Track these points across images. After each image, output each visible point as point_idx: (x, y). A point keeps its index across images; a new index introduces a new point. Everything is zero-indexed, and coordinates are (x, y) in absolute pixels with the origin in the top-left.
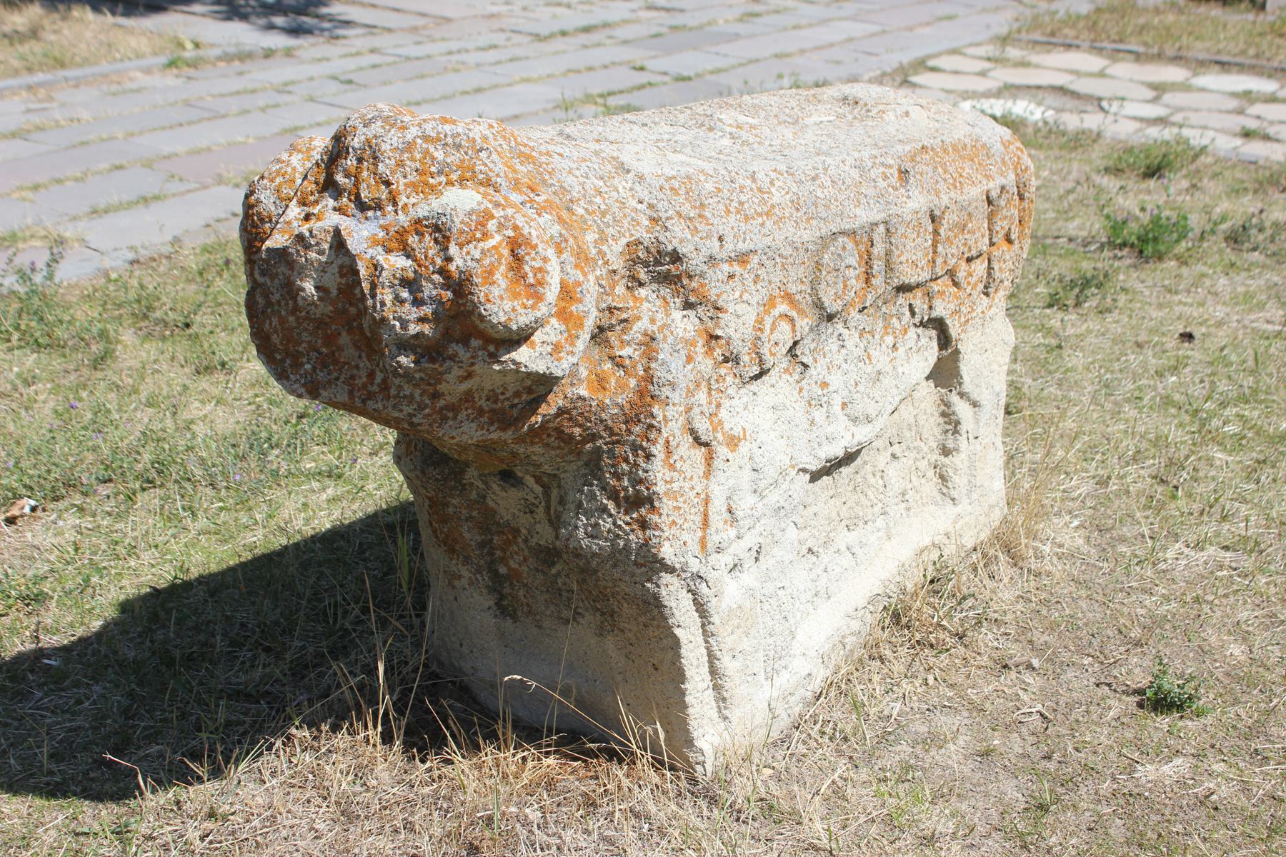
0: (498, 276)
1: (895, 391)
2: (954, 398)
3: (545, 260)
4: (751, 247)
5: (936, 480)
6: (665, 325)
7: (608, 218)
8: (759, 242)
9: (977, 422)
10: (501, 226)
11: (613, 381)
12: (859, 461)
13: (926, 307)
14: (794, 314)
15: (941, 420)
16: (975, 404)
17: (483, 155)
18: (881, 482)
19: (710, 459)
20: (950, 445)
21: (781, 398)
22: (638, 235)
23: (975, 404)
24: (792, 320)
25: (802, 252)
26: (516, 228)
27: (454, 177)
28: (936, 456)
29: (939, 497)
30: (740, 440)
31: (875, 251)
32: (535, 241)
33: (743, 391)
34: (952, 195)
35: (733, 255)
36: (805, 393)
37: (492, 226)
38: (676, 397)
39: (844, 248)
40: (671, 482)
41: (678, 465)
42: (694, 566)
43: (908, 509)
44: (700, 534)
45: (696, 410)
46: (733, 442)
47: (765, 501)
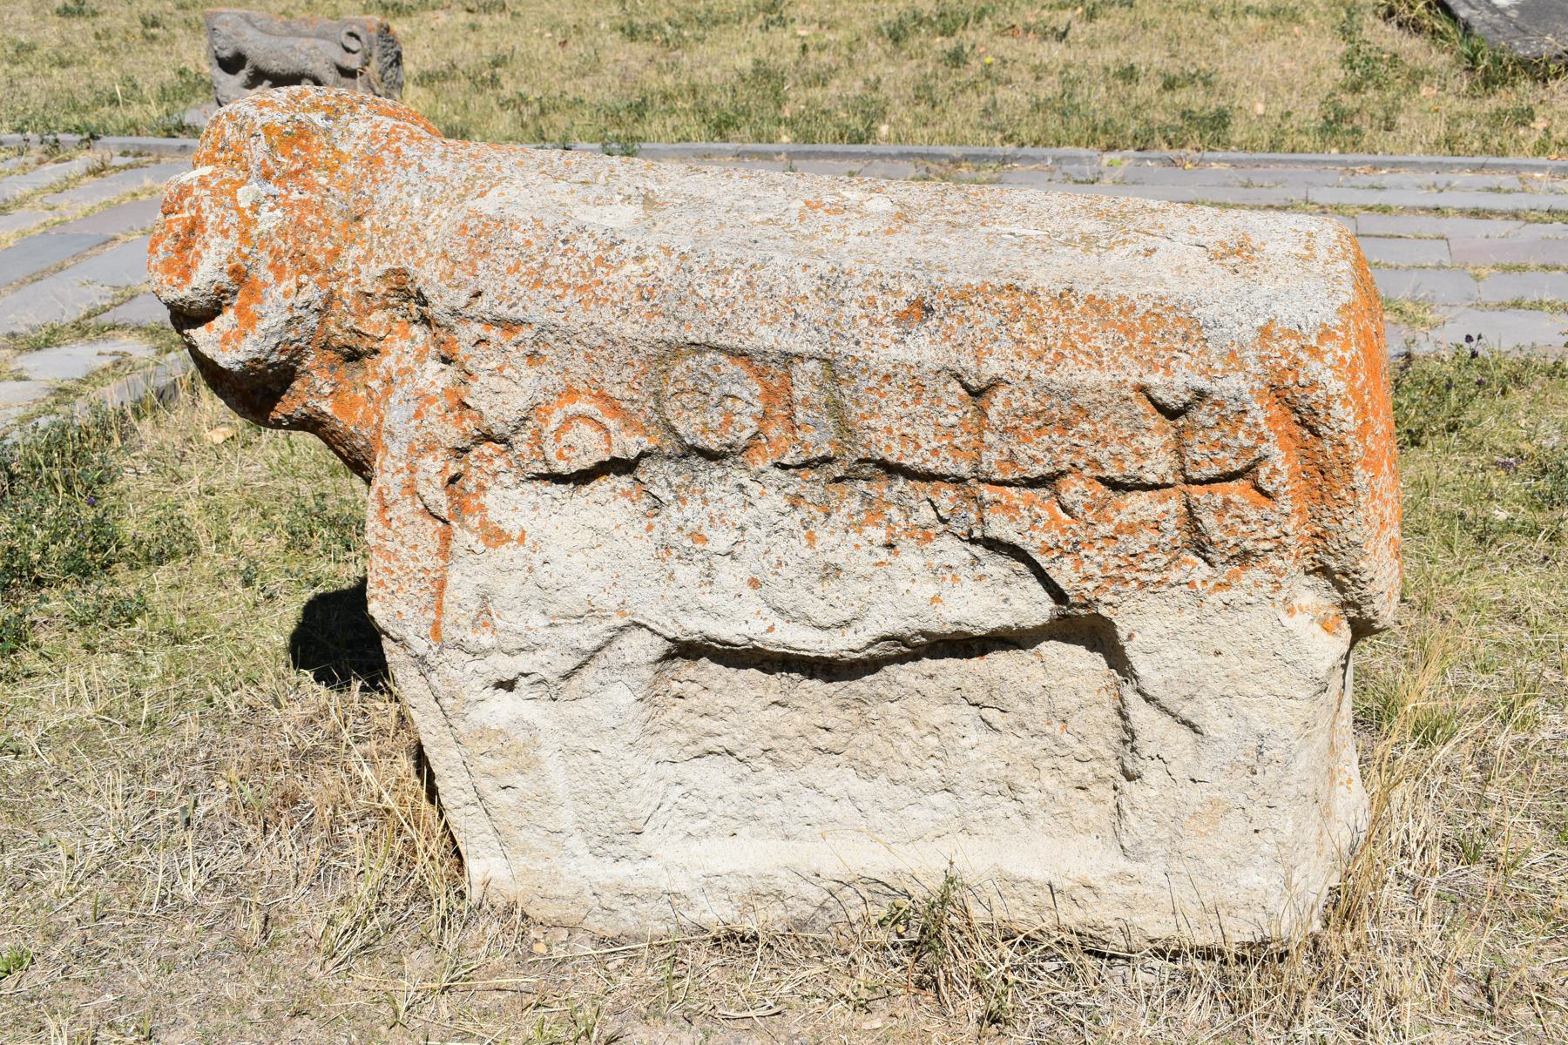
0: (160, 248)
1: (890, 610)
2: (1132, 698)
3: (206, 245)
4: (521, 316)
5: (1111, 804)
6: (408, 371)
7: (387, 241)
8: (539, 315)
9: (1198, 757)
10: (191, 205)
11: (361, 409)
12: (861, 685)
13: (973, 516)
14: (611, 424)
15: (1118, 719)
16: (1193, 727)
17: (253, 140)
18: (932, 741)
19: (446, 539)
20: (1129, 766)
21: (604, 523)
22: (405, 265)
23: (1193, 727)
24: (602, 427)
25: (625, 351)
26: (199, 210)
27: (230, 156)
28: (1113, 770)
29: (1110, 834)
30: (509, 539)
31: (798, 394)
32: (208, 226)
33: (528, 486)
34: (1022, 366)
35: (488, 316)
36: (656, 534)
37: (186, 202)
38: (394, 449)
39: (717, 369)
40: (382, 537)
41: (394, 524)
42: (420, 647)
43: (1027, 816)
44: (431, 615)
45: (420, 475)
46: (495, 536)
47: (556, 630)
